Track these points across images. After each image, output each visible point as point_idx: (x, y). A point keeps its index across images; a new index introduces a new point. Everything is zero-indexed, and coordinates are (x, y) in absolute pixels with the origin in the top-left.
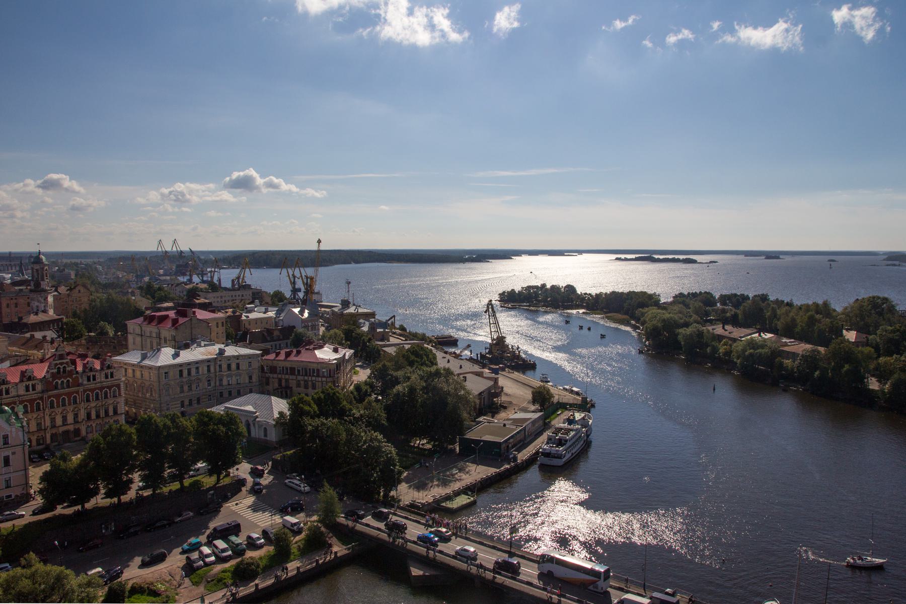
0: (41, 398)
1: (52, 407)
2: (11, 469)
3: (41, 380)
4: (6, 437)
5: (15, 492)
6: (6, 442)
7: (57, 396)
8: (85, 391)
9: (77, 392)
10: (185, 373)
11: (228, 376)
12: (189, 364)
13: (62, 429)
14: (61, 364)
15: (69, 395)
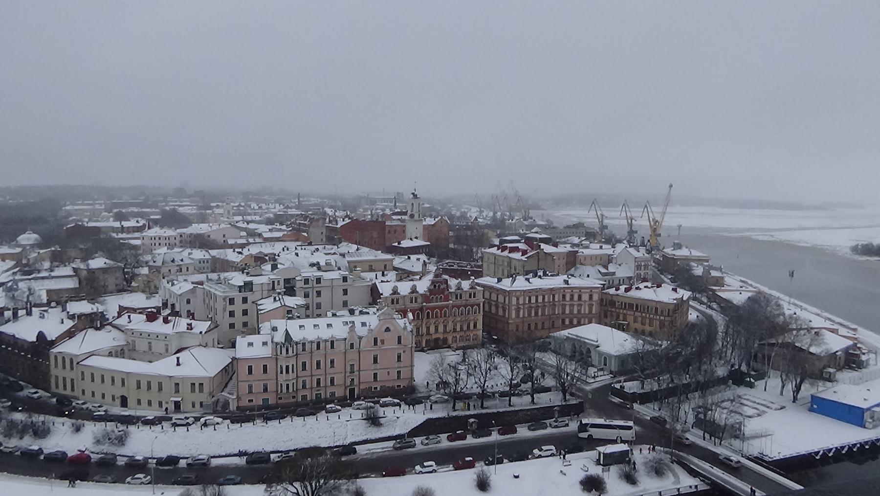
0: (421, 309)
1: (428, 317)
2: (402, 365)
3: (422, 295)
4: (399, 338)
5: (403, 384)
6: (399, 342)
7: (432, 309)
8: (453, 307)
9: (447, 308)
10: (568, 298)
11: (578, 305)
12: (552, 289)
13: (434, 337)
14: (437, 282)
15: (441, 308)
